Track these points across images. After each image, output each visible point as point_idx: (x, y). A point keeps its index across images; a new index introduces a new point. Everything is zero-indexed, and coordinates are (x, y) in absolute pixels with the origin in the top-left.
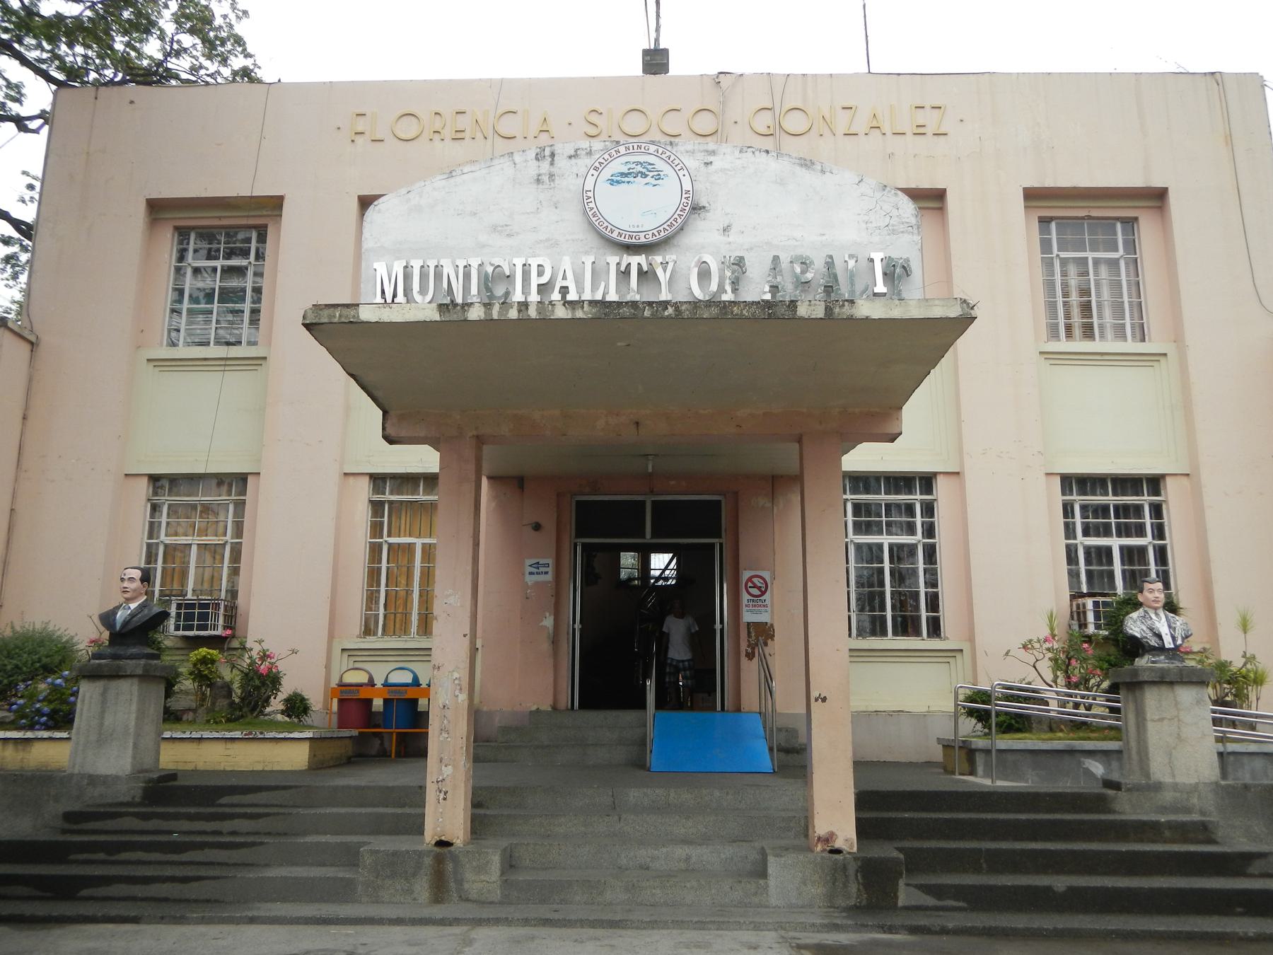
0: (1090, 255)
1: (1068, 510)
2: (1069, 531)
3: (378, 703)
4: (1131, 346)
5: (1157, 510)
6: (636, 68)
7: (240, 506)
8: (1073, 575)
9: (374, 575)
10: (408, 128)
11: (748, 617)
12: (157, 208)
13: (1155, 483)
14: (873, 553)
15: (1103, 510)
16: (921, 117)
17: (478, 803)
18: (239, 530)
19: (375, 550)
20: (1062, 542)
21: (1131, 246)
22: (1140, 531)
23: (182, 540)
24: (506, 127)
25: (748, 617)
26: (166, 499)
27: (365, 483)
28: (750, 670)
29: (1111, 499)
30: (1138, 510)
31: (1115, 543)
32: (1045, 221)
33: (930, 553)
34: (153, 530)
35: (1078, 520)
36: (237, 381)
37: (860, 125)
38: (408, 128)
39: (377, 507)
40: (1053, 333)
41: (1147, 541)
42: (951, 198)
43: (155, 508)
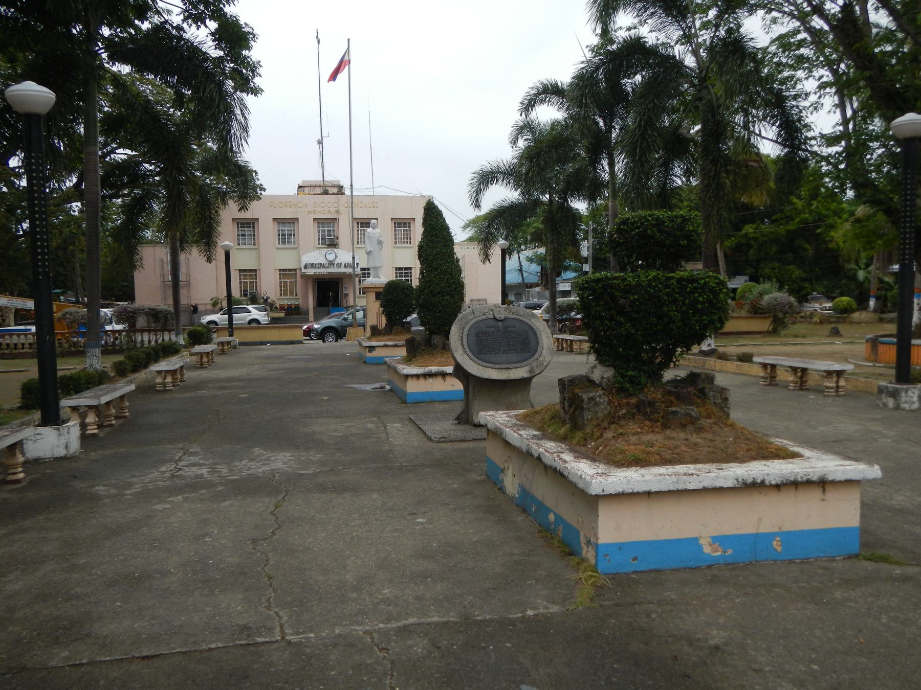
0: (403, 229)
1: (396, 273)
3: (286, 307)
4: (408, 245)
5: (411, 273)
7: (256, 275)
9: (281, 286)
10: (281, 205)
11: (344, 292)
13: (411, 269)
15: (402, 273)
16: (374, 204)
17: (314, 318)
18: (256, 279)
19: (281, 282)
21: (410, 227)
24: (299, 205)
25: (344, 292)
26: (242, 274)
27: (278, 271)
28: (345, 300)
32: (395, 223)
34: (240, 279)
36: (254, 252)
37: (363, 206)
38: (281, 205)
39: (280, 275)
41: (409, 278)
43: (240, 275)
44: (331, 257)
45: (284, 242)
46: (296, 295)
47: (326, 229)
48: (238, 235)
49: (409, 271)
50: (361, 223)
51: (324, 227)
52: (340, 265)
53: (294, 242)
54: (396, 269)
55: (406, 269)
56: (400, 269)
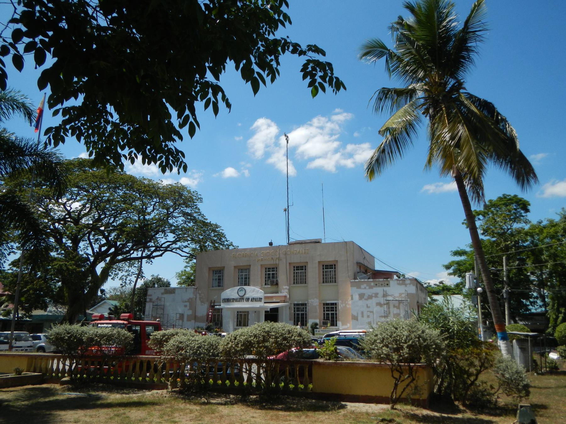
1: (324, 308)
2: (324, 311)
5: (336, 308)
6: (268, 245)
8: (324, 317)
12: (210, 268)
14: (298, 314)
15: (329, 308)
20: (323, 312)
22: (334, 311)
23: (215, 314)
29: (330, 306)
30: (333, 308)
31: (330, 312)
33: (306, 314)
35: (325, 309)
40: (323, 282)
41: (334, 312)
42: (309, 263)
44: (241, 293)
47: (271, 273)
48: (213, 279)
49: (334, 306)
50: (297, 267)
51: (268, 271)
52: (248, 299)
53: (249, 284)
54: (324, 304)
55: (332, 304)
56: (327, 304)
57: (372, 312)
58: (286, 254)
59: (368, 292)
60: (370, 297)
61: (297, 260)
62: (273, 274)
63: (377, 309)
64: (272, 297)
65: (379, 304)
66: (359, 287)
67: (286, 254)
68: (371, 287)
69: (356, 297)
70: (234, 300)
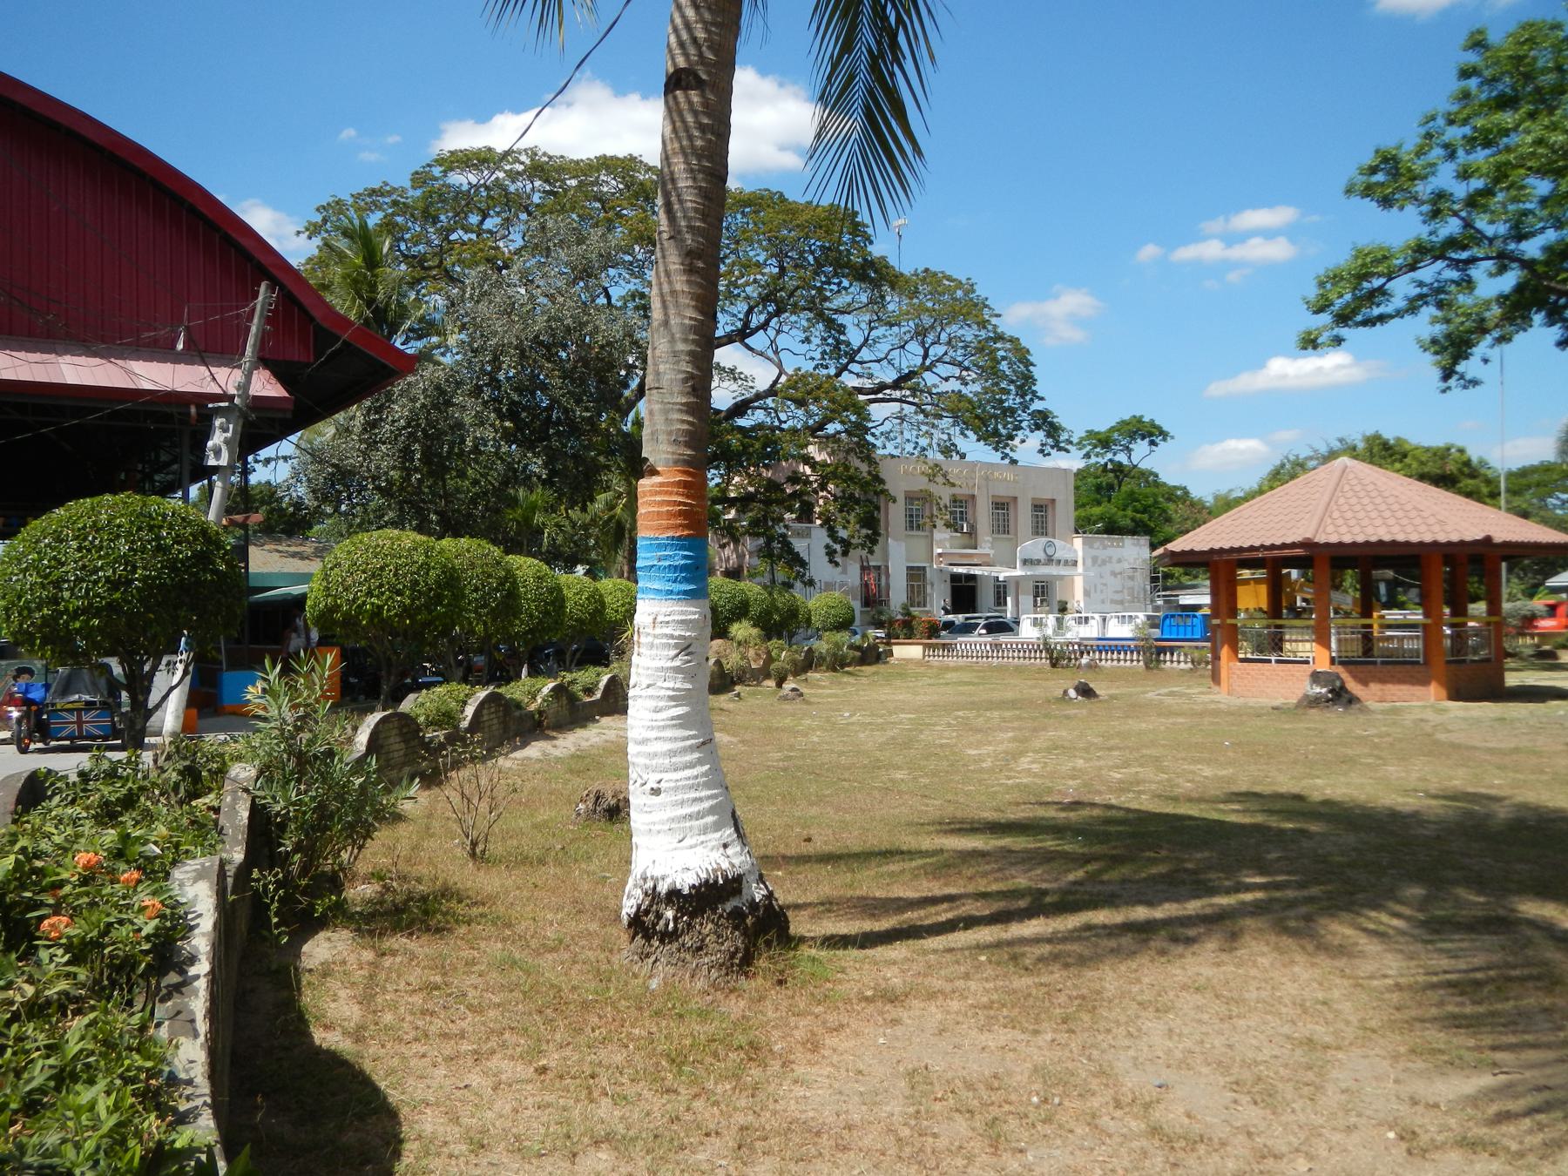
42: (1019, 500)
44: (1050, 551)
45: (912, 528)
46: (925, 606)
52: (1059, 562)
57: (1105, 585)
58: (987, 479)
59: (1103, 554)
60: (1104, 563)
61: (1003, 492)
62: (961, 512)
63: (1111, 580)
64: (971, 555)
65: (1114, 574)
66: (1091, 547)
67: (987, 479)
68: (1105, 548)
69: (1089, 562)
70: (1039, 562)
